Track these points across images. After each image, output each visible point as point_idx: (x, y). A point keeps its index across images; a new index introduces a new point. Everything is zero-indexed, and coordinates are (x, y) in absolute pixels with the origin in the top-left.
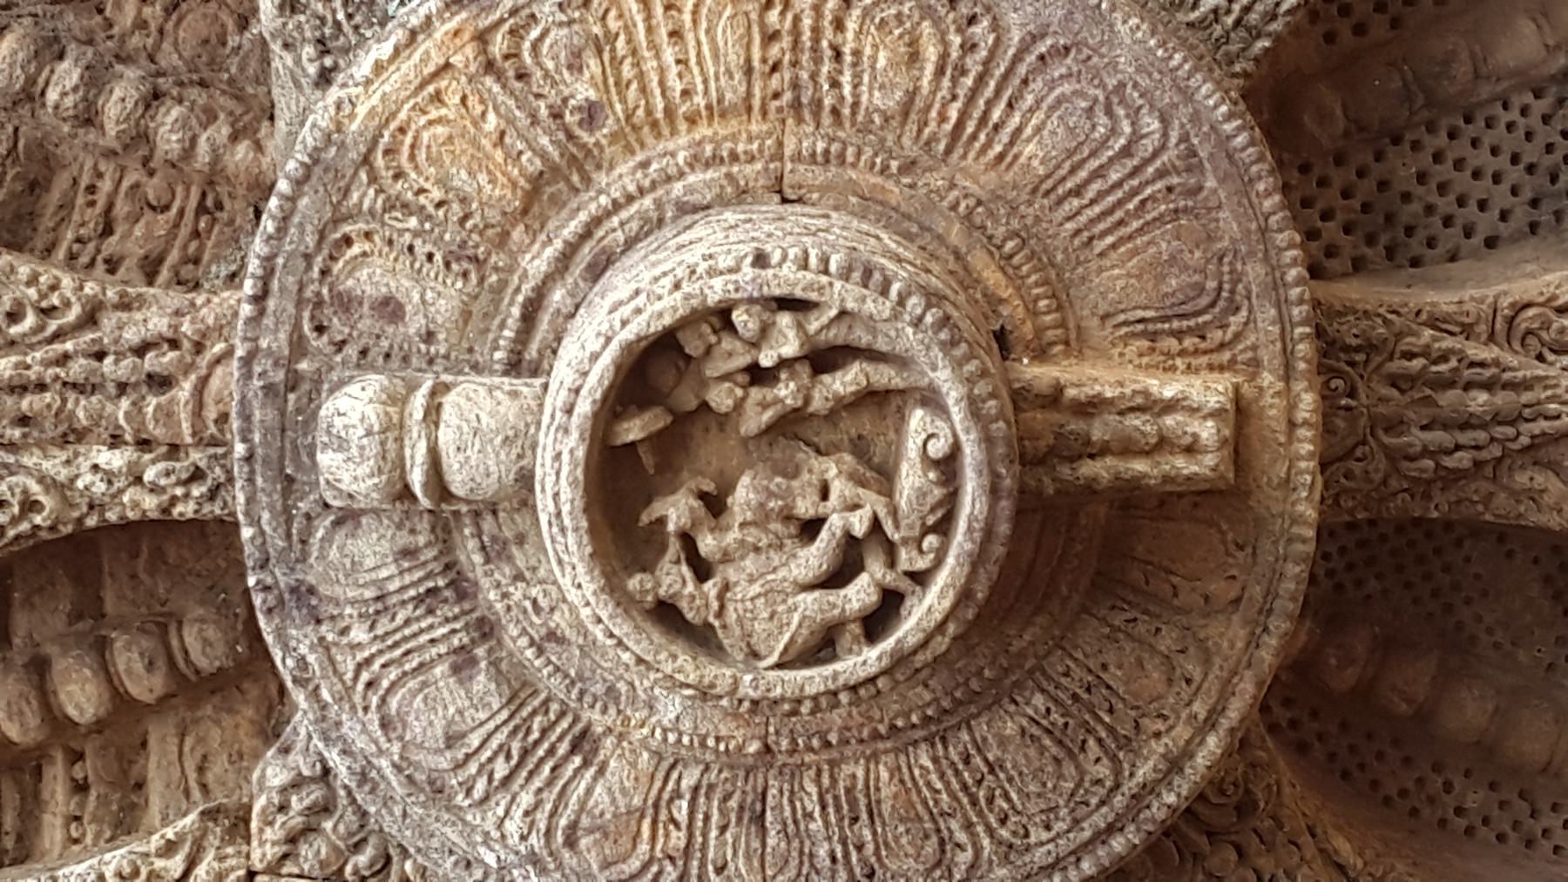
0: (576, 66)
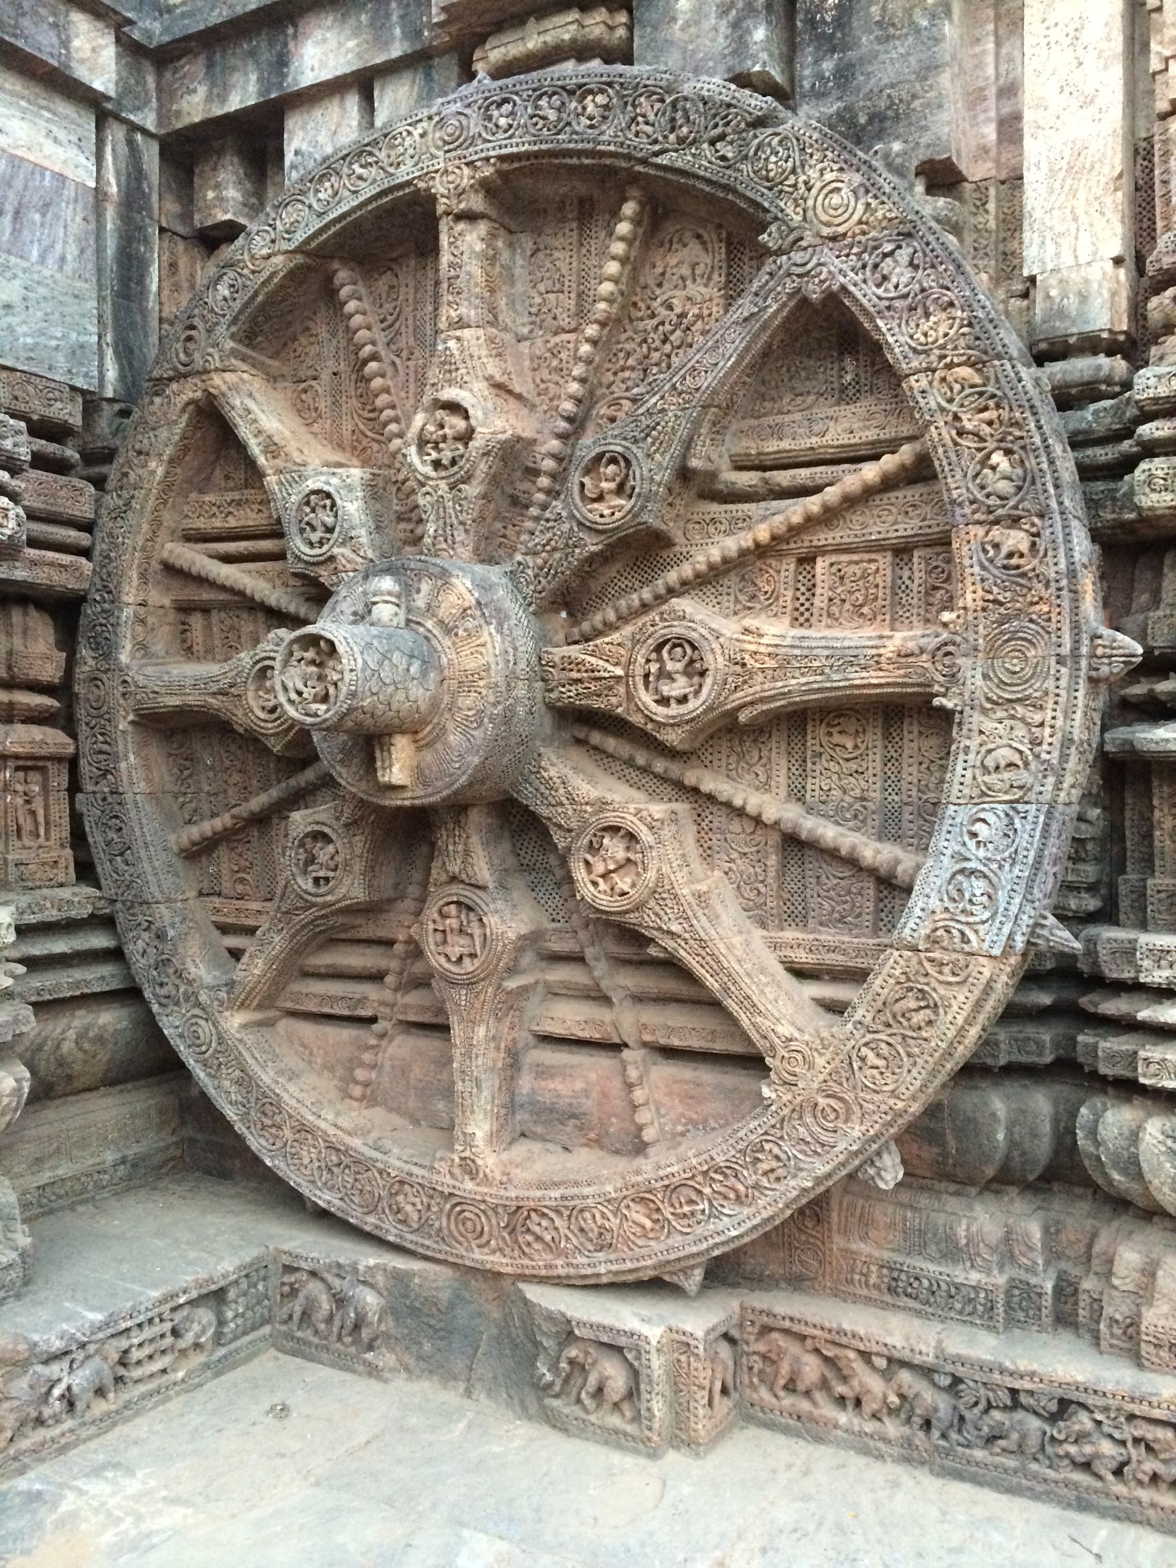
0: (466, 630)
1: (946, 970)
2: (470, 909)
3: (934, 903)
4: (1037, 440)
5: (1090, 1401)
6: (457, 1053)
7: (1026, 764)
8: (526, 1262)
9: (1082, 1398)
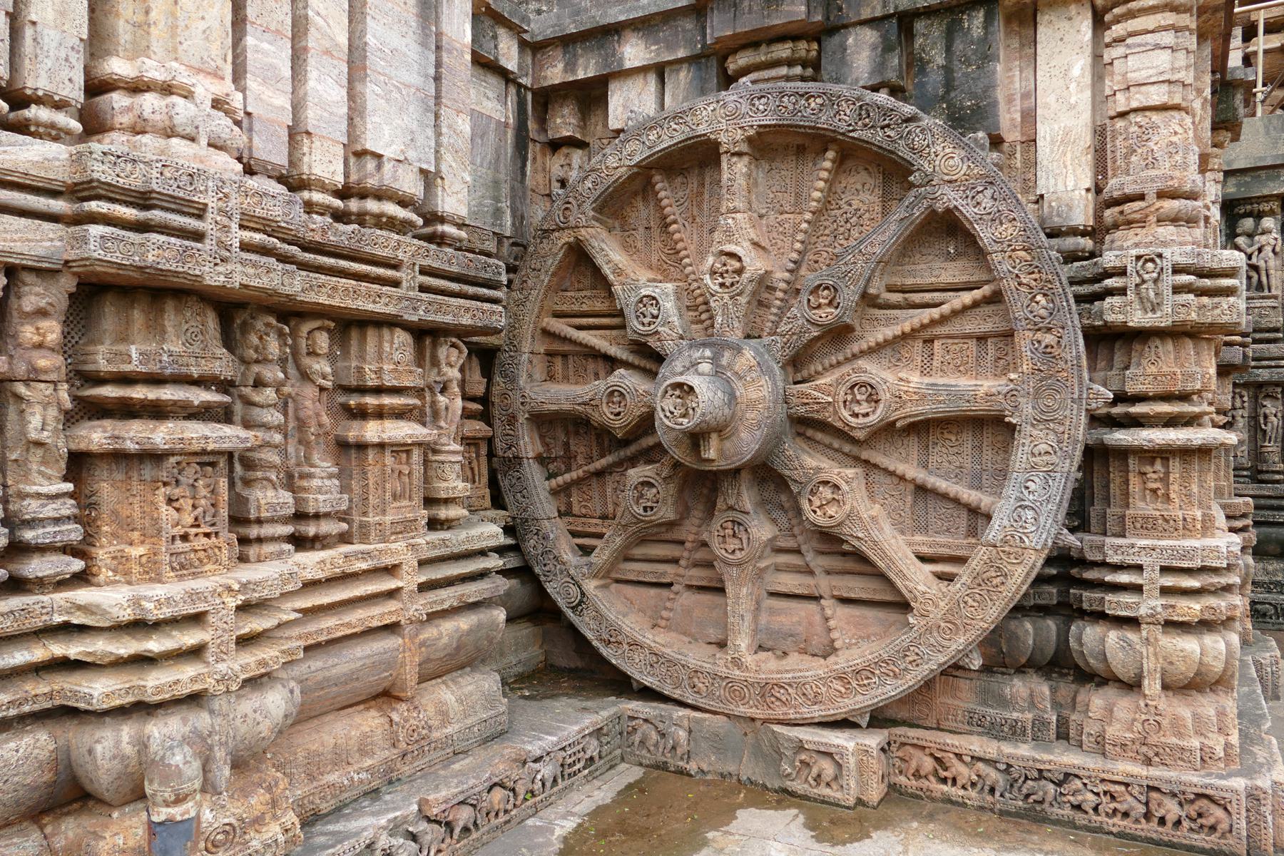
1: (1012, 557)
2: (739, 524)
3: (1006, 522)
4: (1060, 290)
5: (1081, 773)
6: (729, 601)
7: (1055, 452)
8: (771, 712)
9: (1076, 772)
